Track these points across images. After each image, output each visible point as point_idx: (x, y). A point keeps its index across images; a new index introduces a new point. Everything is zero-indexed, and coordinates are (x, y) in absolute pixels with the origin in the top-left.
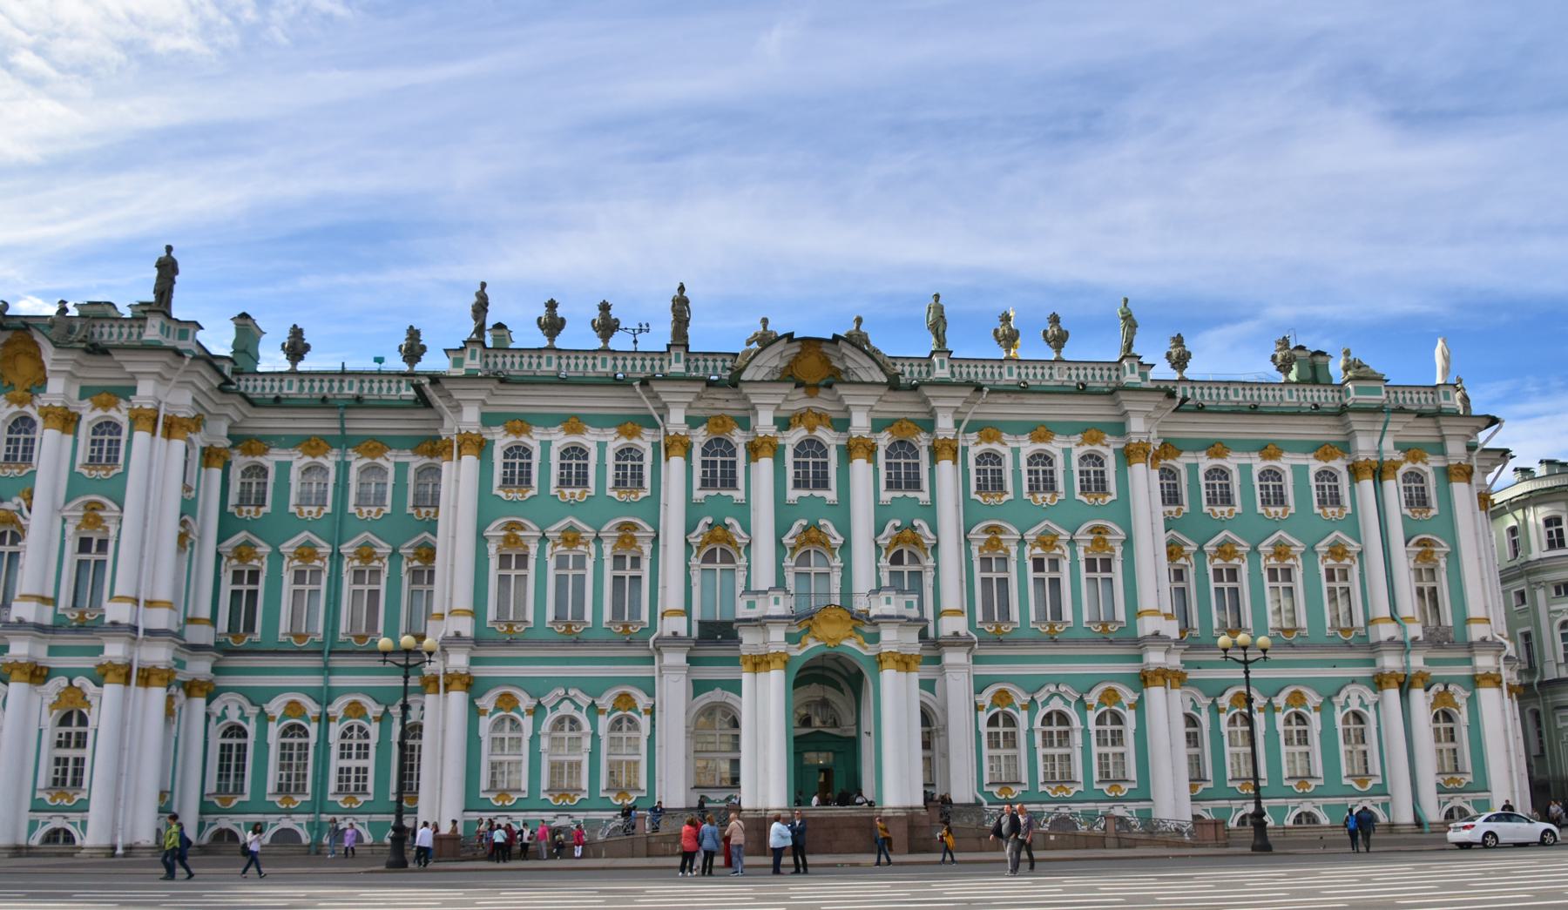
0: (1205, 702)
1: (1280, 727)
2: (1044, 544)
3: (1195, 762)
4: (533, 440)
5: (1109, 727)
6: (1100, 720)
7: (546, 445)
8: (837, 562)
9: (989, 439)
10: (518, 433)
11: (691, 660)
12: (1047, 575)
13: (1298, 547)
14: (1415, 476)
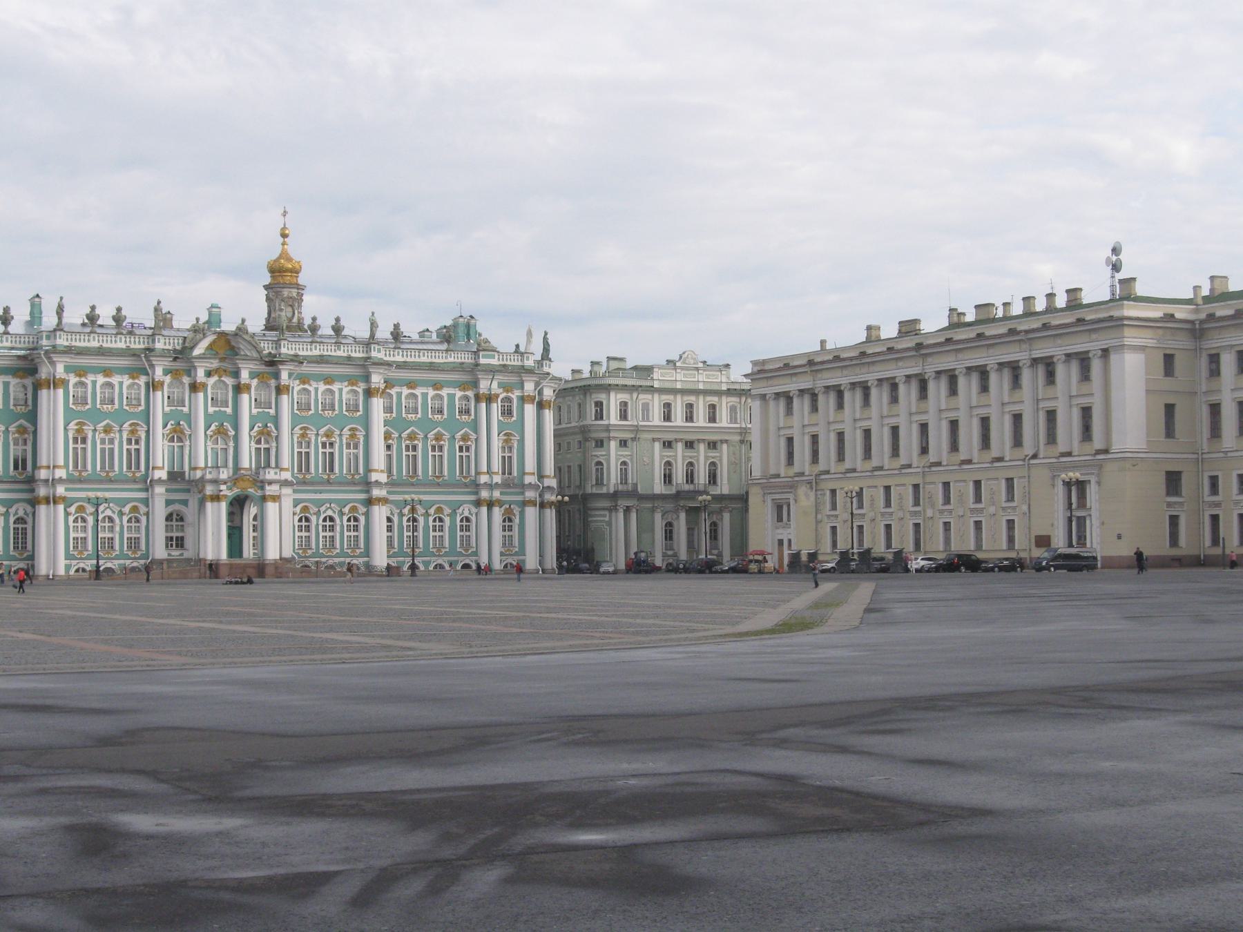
0: (396, 511)
1: (431, 523)
2: (327, 436)
3: (390, 539)
4: (89, 379)
5: (352, 523)
6: (349, 520)
7: (94, 383)
8: (231, 444)
9: (304, 383)
10: (80, 376)
11: (167, 490)
12: (328, 450)
13: (447, 435)
14: (509, 400)
